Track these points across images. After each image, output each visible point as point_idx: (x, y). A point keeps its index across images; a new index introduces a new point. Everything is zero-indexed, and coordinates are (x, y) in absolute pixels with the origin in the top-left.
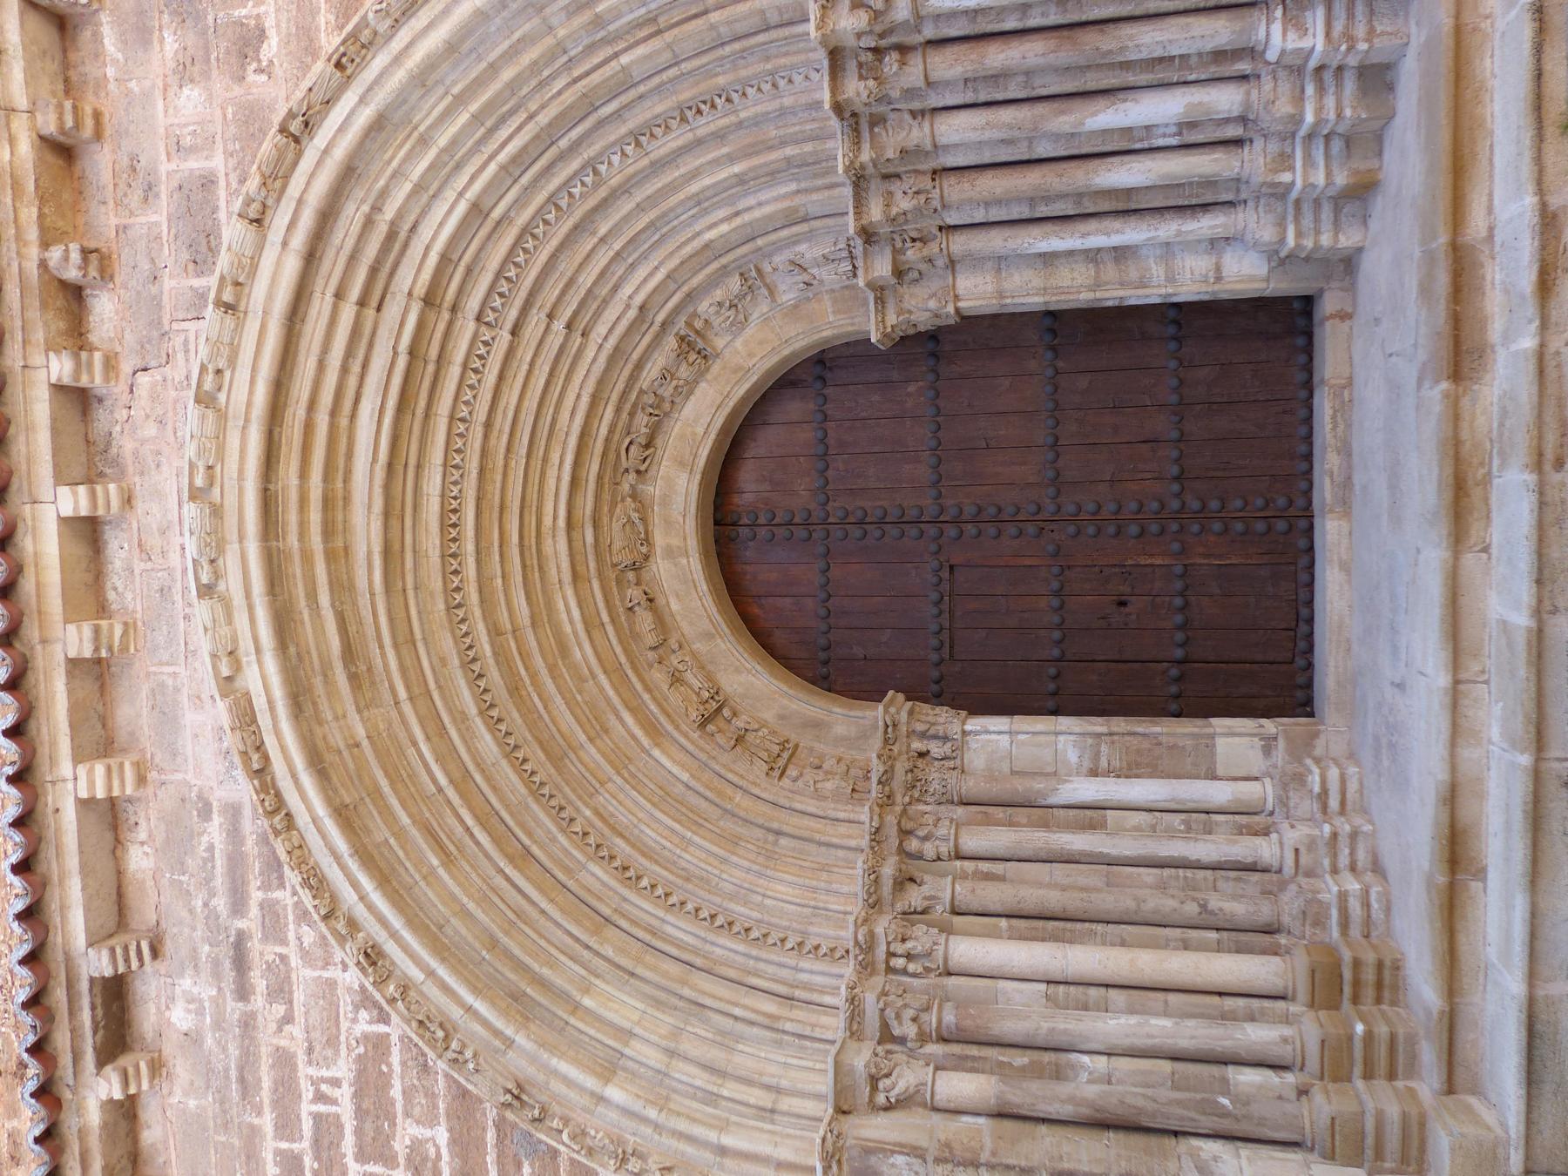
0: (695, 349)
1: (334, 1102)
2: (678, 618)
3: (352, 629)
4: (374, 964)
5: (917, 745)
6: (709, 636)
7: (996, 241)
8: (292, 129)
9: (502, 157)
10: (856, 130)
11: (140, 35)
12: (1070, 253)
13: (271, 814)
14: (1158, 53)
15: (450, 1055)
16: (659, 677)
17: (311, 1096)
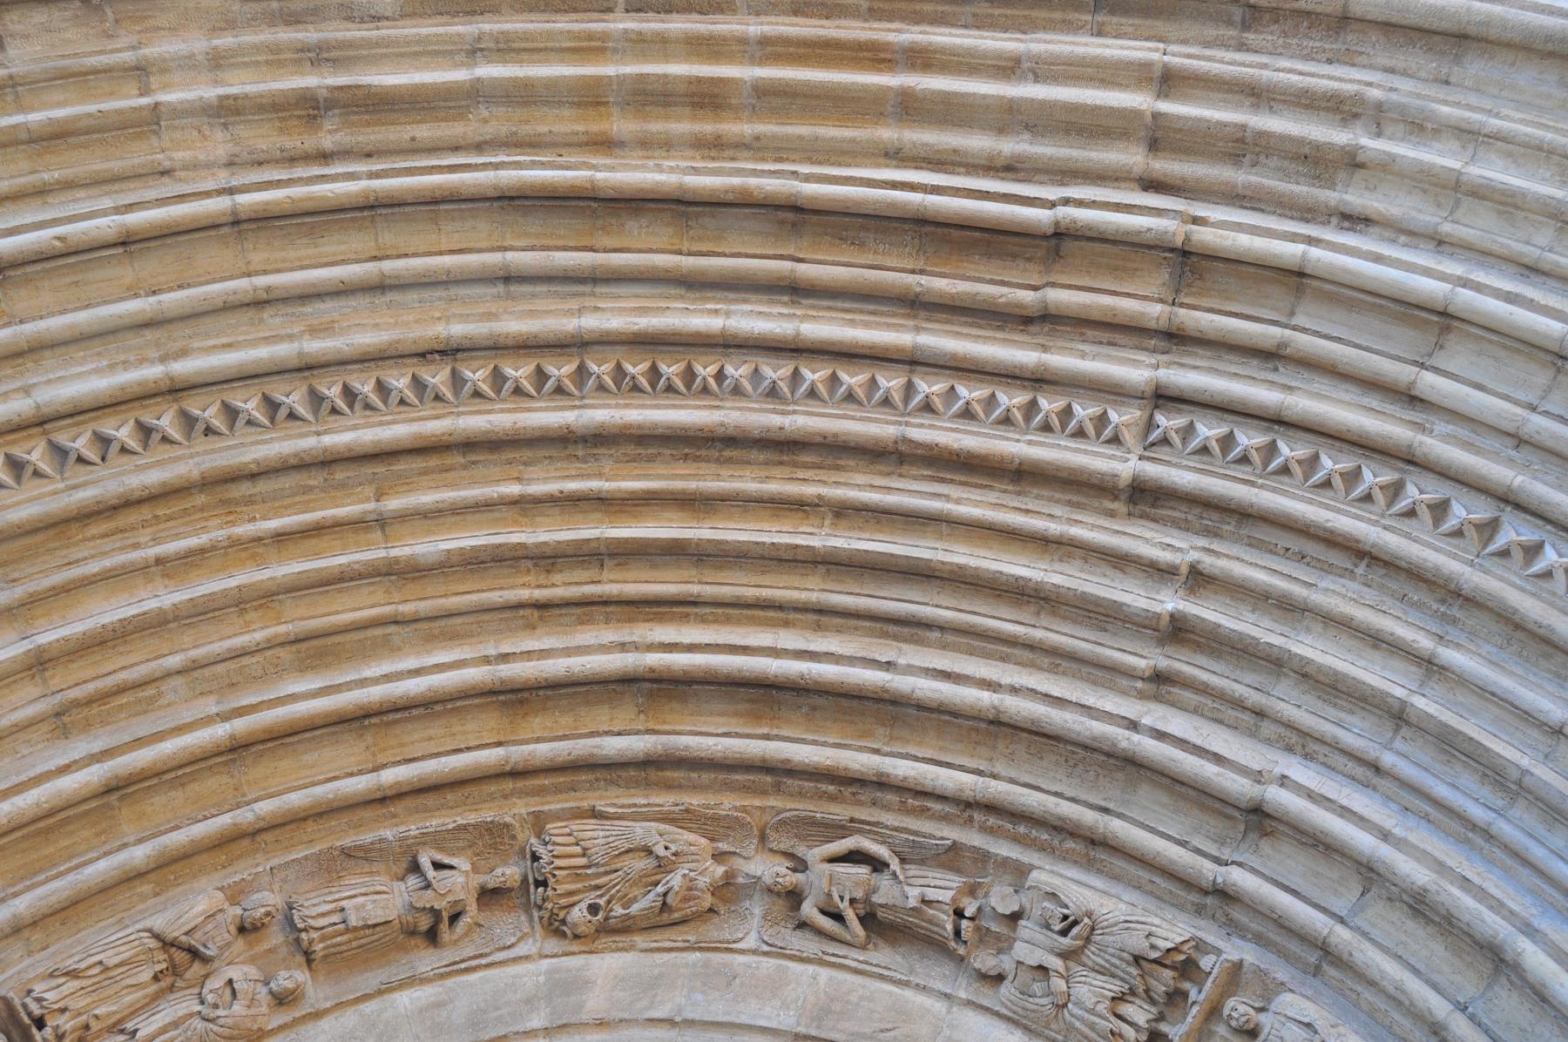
16: (194, 906)
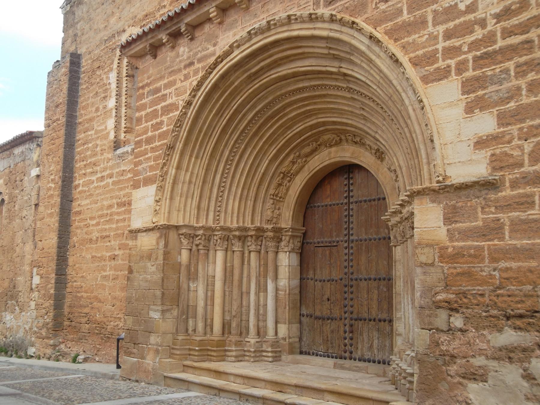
3: (261, 73)
4: (188, 104)
13: (210, 68)
15: (174, 129)
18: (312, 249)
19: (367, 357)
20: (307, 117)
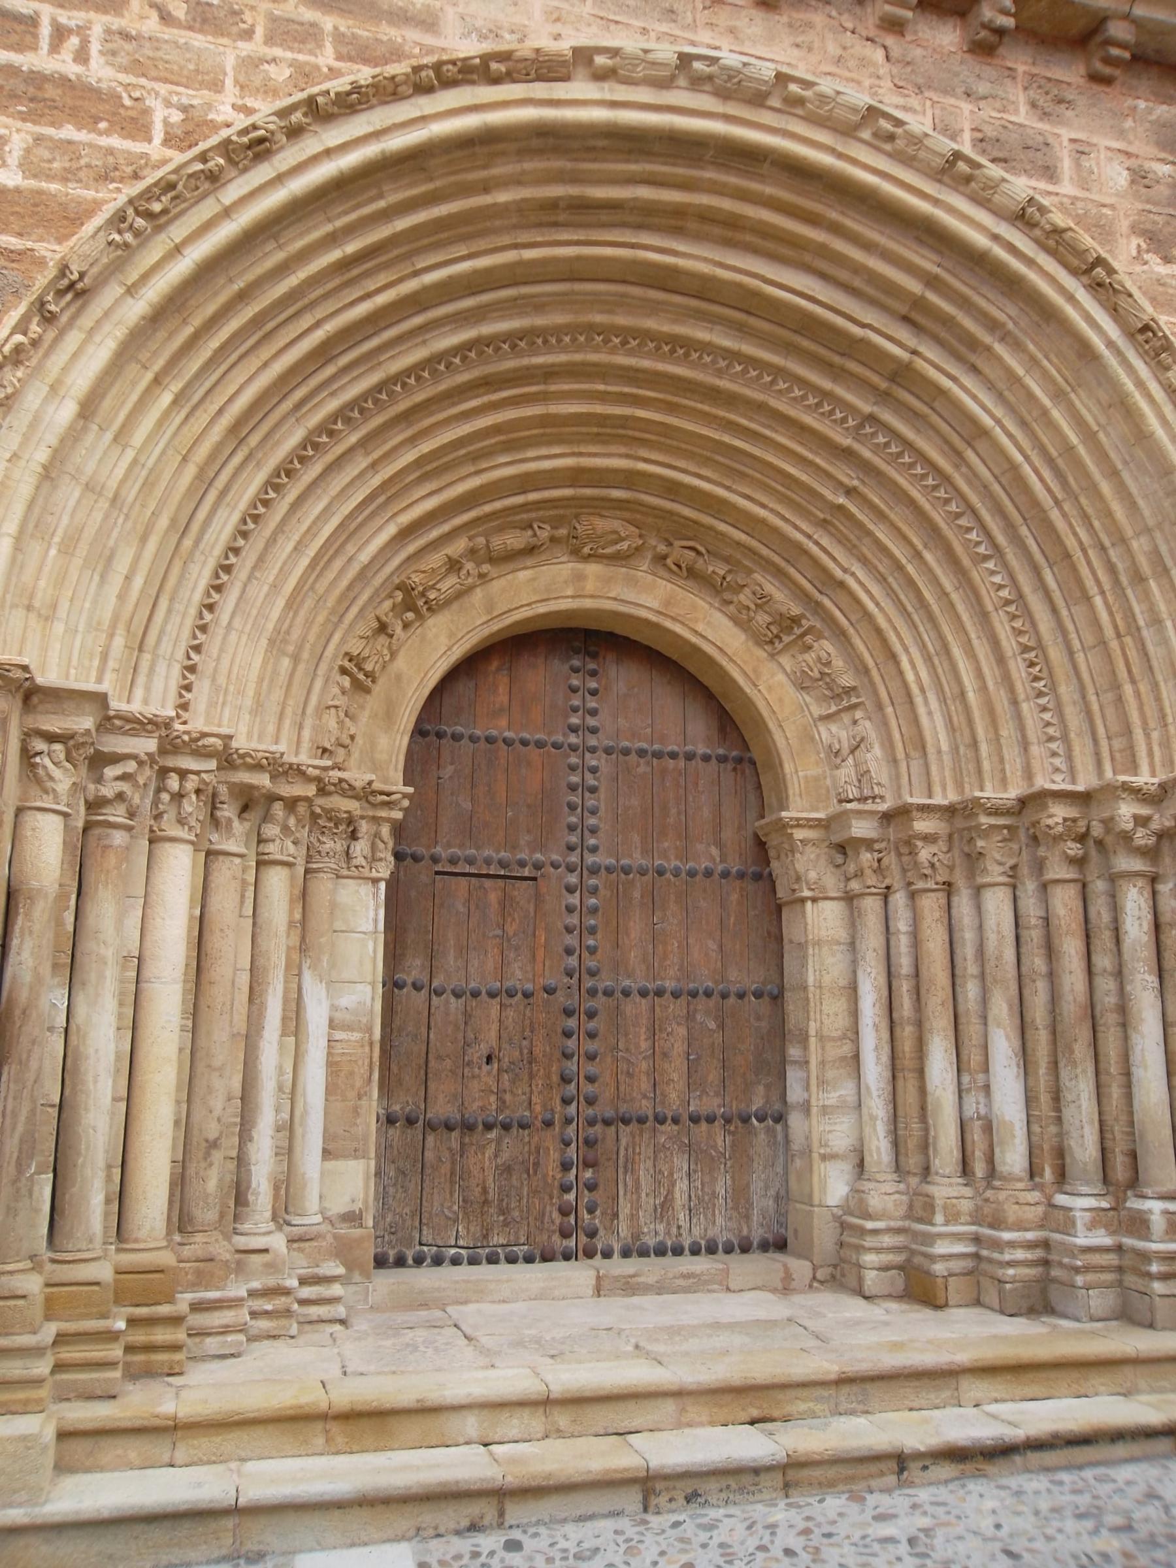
0: (781, 633)
1: (55, 48)
2: (509, 577)
3: (604, 217)
4: (249, 147)
5: (364, 827)
6: (490, 606)
7: (872, 941)
8: (1099, 270)
9: (1027, 469)
10: (1008, 812)
11: (1174, 142)
12: (855, 1013)
13: (437, 67)
14: (1068, 1096)
17: (63, 20)
18: (424, 878)
19: (651, 1242)
20: (598, 439)
